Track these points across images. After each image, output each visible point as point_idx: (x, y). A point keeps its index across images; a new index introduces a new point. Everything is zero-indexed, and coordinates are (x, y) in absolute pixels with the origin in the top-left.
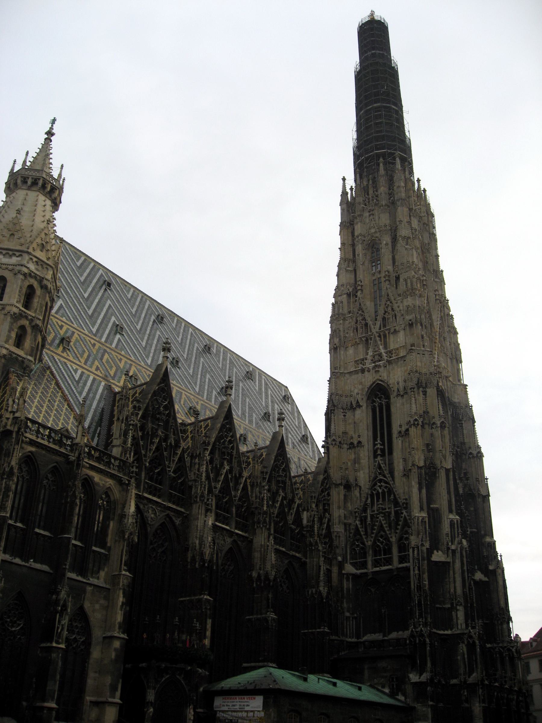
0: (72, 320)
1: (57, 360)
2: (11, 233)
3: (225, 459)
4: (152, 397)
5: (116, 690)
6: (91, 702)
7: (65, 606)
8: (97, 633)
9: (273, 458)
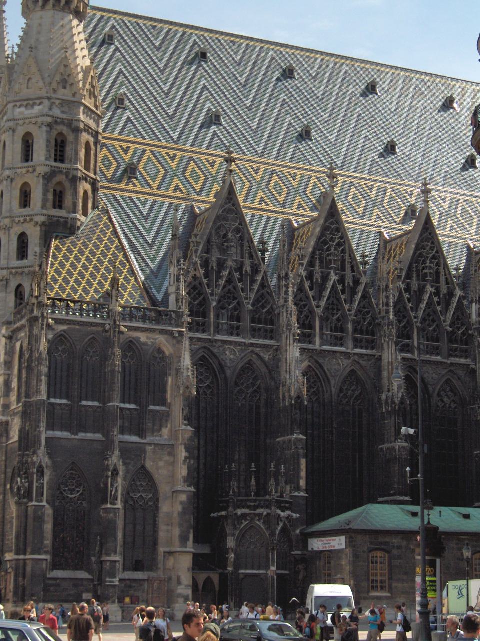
0: (144, 133)
1: (120, 198)
2: (29, 76)
3: (331, 268)
4: (215, 223)
5: (188, 539)
6: (165, 552)
7: (115, 472)
8: (164, 489)
9: (414, 246)
